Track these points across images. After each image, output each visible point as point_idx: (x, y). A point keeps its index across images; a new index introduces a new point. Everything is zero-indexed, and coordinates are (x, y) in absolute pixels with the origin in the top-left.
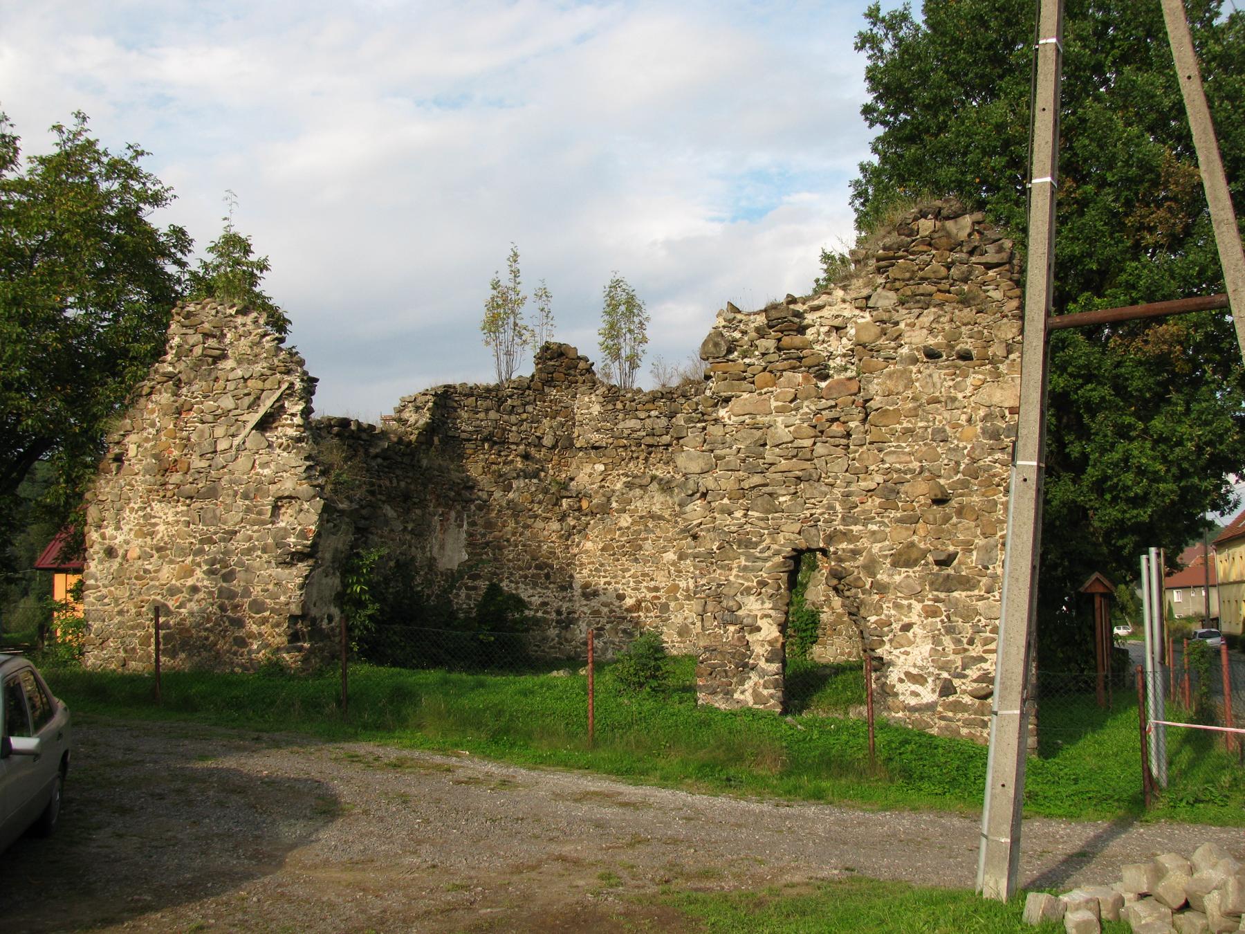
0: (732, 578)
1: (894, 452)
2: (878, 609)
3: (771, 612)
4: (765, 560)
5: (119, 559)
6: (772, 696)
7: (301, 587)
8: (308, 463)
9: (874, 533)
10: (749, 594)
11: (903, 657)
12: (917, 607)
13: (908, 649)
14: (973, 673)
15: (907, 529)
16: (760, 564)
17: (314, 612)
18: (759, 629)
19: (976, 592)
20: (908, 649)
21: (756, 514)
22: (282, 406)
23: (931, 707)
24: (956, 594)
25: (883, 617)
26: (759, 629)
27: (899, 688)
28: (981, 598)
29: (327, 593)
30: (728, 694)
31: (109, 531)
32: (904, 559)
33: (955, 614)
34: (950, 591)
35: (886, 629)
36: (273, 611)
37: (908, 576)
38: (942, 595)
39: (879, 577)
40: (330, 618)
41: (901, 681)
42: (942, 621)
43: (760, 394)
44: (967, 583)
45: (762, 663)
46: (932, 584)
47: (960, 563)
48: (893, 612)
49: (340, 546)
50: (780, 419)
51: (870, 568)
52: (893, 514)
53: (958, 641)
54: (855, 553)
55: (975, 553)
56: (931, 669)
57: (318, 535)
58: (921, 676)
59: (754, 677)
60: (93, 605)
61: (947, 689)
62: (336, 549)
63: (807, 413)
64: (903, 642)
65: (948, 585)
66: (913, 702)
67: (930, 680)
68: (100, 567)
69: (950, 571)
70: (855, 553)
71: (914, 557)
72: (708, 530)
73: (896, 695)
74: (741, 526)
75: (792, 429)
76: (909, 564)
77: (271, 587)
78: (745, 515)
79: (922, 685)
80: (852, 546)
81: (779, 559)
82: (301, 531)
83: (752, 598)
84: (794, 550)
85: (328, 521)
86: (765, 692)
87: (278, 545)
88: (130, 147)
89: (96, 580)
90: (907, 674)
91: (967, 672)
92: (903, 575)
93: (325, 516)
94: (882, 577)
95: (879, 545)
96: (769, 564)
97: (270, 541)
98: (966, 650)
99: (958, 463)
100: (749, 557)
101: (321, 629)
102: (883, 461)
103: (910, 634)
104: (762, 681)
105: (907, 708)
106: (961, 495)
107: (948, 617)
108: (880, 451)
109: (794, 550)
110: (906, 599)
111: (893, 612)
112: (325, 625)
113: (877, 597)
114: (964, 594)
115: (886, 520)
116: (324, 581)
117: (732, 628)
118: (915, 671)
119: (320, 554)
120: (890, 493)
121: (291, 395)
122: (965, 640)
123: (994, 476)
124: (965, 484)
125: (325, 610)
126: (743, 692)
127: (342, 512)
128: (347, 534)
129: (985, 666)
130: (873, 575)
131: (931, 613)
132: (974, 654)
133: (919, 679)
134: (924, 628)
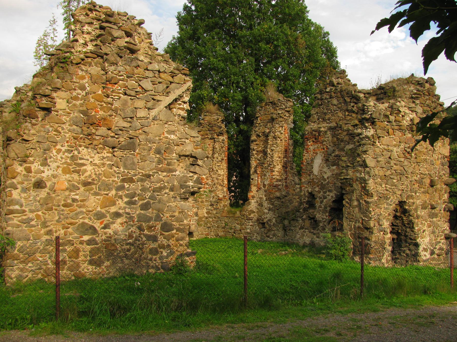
0: (382, 212)
2: (417, 224)
4: (391, 205)
5: (47, 190)
9: (418, 196)
19: (438, 219)
21: (389, 186)
23: (428, 260)
28: (439, 221)
30: (380, 260)
31: (35, 166)
32: (424, 208)
36: (178, 230)
38: (431, 220)
39: (418, 212)
43: (390, 138)
50: (395, 149)
51: (416, 210)
52: (422, 190)
54: (413, 203)
60: (18, 226)
61: (432, 253)
63: (402, 148)
66: (424, 258)
68: (23, 195)
69: (433, 211)
75: (398, 153)
76: (425, 208)
77: (176, 214)
78: (386, 187)
82: (198, 178)
83: (385, 220)
86: (389, 258)
87: (182, 187)
89: (21, 206)
91: (437, 247)
96: (391, 207)
97: (176, 183)
100: (387, 204)
103: (424, 234)
108: (419, 166)
114: (436, 219)
117: (382, 233)
120: (420, 182)
130: (416, 212)
131: (429, 226)
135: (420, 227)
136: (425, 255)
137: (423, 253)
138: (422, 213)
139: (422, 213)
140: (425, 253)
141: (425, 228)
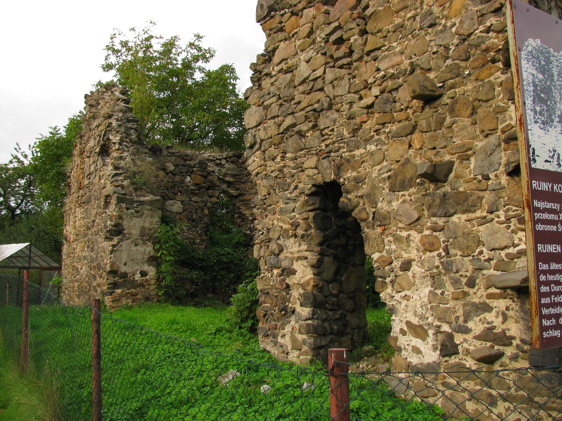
1: (386, 57)
3: (307, 254)
6: (304, 342)
8: (115, 172)
10: (289, 237)
11: (404, 303)
12: (415, 236)
13: (408, 293)
14: (476, 326)
15: (402, 143)
16: (291, 205)
17: (123, 269)
18: (294, 272)
19: (478, 214)
20: (408, 293)
22: (109, 139)
24: (455, 218)
25: (384, 253)
26: (294, 272)
27: (403, 341)
28: (484, 221)
29: (140, 257)
33: (454, 245)
34: (448, 215)
35: (387, 268)
37: (404, 201)
38: (441, 222)
39: (379, 205)
40: (144, 274)
41: (403, 332)
42: (439, 255)
44: (466, 203)
45: (298, 309)
46: (430, 207)
47: (457, 177)
48: (393, 247)
49: (147, 225)
53: (456, 282)
54: (359, 181)
55: (472, 159)
56: (430, 320)
58: (421, 326)
59: (293, 319)
61: (448, 348)
62: (143, 228)
64: (404, 284)
65: (446, 206)
66: (414, 360)
67: (431, 332)
69: (447, 188)
70: (359, 181)
71: (408, 176)
72: (262, 179)
73: (400, 350)
74: (281, 170)
79: (424, 339)
80: (355, 174)
81: (303, 198)
84: (314, 185)
88: (195, 36)
90: (408, 323)
91: (470, 325)
92: (401, 200)
93: (124, 205)
94: (382, 206)
95: (378, 167)
98: (465, 294)
99: (447, 48)
101: (134, 280)
102: (378, 70)
104: (297, 326)
105: (409, 367)
106: (453, 87)
107: (446, 250)
109: (314, 185)
110: (407, 230)
111: (393, 247)
112: (138, 277)
113: (379, 230)
114: (464, 217)
115: (383, 137)
116: (134, 248)
117: (276, 271)
118: (415, 321)
119: (126, 231)
120: (385, 105)
122: (464, 280)
123: (487, 50)
124: (455, 71)
125: (137, 267)
126: (283, 336)
127: (142, 203)
128: (152, 216)
129: (490, 316)
130: (374, 204)
132: (476, 300)
133: (419, 331)
134: (422, 266)
135: (389, 252)
136: (417, 350)
137: (407, 342)
138: (391, 203)
139: (391, 203)
140: (417, 342)
141: (414, 254)
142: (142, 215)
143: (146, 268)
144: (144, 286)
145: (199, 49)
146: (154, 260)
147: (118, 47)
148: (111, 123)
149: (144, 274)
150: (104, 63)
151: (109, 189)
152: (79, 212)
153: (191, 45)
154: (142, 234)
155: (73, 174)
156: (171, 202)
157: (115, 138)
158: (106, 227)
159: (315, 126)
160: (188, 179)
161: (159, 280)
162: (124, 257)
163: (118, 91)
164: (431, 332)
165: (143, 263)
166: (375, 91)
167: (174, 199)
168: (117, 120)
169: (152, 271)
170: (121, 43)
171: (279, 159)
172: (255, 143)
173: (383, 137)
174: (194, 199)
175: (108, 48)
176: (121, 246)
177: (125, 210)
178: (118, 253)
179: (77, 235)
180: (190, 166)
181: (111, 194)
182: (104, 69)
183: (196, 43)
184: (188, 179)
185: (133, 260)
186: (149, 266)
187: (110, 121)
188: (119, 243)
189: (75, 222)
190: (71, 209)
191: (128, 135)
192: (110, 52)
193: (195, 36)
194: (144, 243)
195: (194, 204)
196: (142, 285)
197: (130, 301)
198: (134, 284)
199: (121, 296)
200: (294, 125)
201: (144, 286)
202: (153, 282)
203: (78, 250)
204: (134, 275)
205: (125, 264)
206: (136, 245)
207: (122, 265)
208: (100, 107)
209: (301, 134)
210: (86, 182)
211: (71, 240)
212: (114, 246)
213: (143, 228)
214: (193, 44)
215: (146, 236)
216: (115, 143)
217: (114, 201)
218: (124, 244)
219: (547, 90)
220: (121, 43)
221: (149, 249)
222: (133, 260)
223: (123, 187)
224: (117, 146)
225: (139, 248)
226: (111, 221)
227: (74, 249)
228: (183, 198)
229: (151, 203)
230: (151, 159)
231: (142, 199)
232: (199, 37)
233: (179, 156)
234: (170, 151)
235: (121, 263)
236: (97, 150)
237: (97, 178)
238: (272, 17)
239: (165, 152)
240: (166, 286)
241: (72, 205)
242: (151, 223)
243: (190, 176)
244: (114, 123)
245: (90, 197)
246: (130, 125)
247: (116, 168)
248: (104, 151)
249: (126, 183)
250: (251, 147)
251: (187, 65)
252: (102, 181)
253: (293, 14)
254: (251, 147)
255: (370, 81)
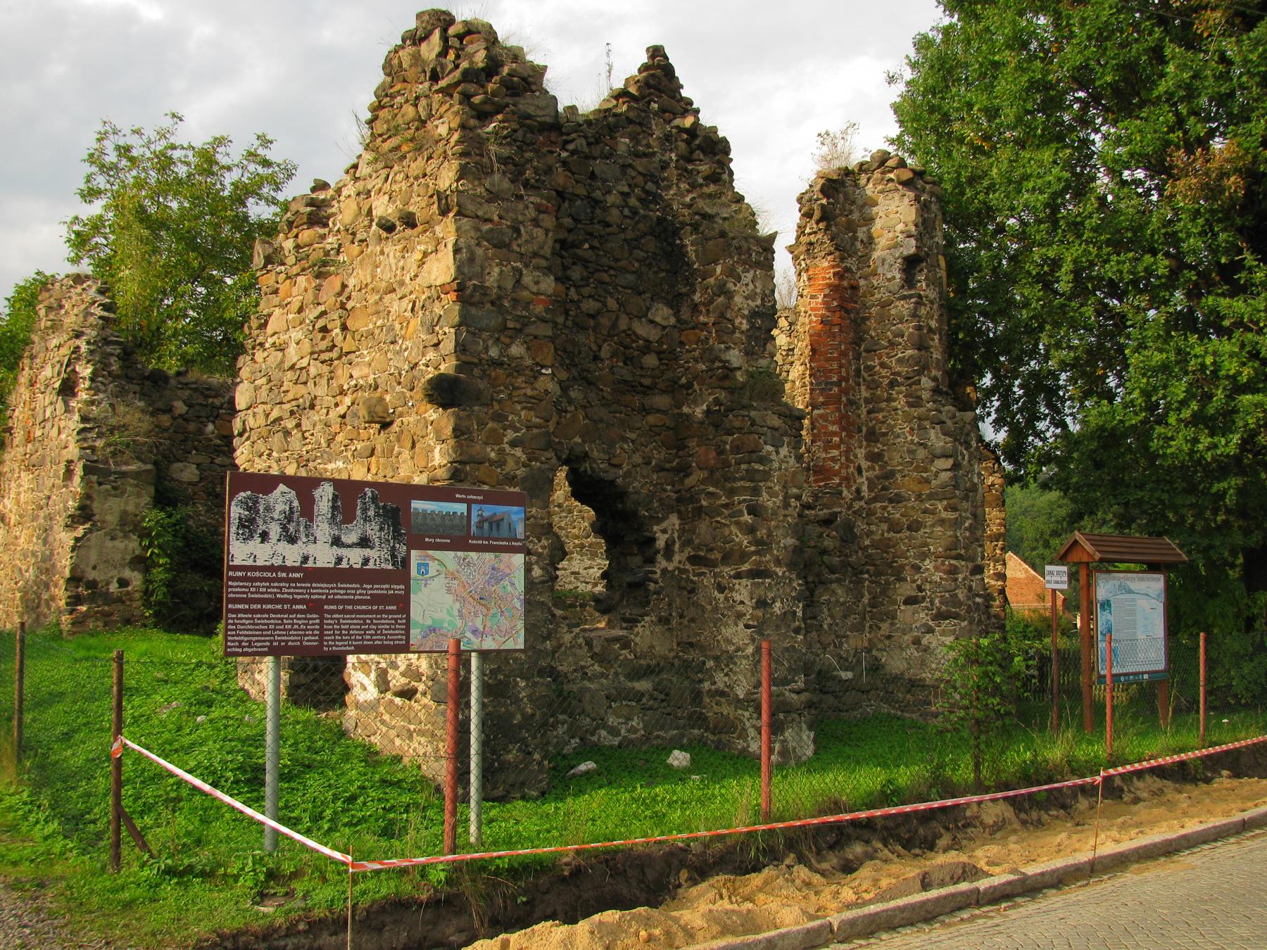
7: (73, 549)
17: (91, 575)
22: (74, 370)
40: (123, 583)
41: (355, 668)
49: (131, 508)
57: (87, 497)
62: (124, 513)
66: (361, 698)
85: (100, 484)
88: (259, 137)
93: (94, 478)
101: (107, 593)
105: (358, 705)
112: (114, 587)
116: (110, 544)
119: (97, 518)
121: (78, 359)
125: (114, 572)
127: (124, 475)
128: (139, 495)
142: (123, 492)
143: (127, 573)
144: (123, 602)
145: (266, 163)
146: (141, 563)
147: (112, 157)
148: (78, 347)
149: (123, 583)
150: (84, 187)
151: (73, 451)
152: (26, 477)
153: (251, 155)
154: (123, 521)
155: (16, 413)
156: (180, 465)
157: (85, 371)
158: (66, 509)
159: (298, 425)
160: (210, 427)
161: (147, 593)
162: (93, 557)
163: (94, 289)
164: (374, 667)
165: (123, 566)
166: (347, 401)
167: (185, 460)
168: (88, 343)
169: (136, 579)
170: (118, 148)
171: (265, 457)
172: (244, 430)
173: (349, 454)
174: (218, 460)
175: (92, 159)
176: (88, 540)
177: (96, 485)
178: (83, 551)
179: (21, 516)
180: (213, 406)
181: (75, 459)
182: (83, 196)
183: (261, 151)
184: (210, 427)
185: (107, 561)
186: (133, 570)
187: (78, 342)
188: (85, 534)
189: (19, 494)
190: (12, 471)
191: (106, 365)
192: (95, 169)
193: (259, 137)
194: (126, 536)
195: (219, 470)
196: (120, 600)
197: (100, 624)
198: (108, 598)
199: (86, 616)
200: (280, 419)
201: (123, 602)
202: (137, 595)
203: (22, 540)
204: (108, 584)
205: (94, 568)
206: (113, 539)
207: (90, 569)
208: (63, 312)
209: (287, 433)
210: (38, 433)
211: (12, 523)
212: (77, 539)
213: (124, 513)
214: (256, 156)
215: (129, 525)
216: (84, 378)
217: (79, 471)
218: (93, 536)
219: (252, 521)
220: (118, 148)
221: (133, 545)
222: (107, 561)
223: (93, 449)
224: (88, 383)
225: (117, 543)
226: (74, 500)
227: (16, 538)
228: (200, 459)
229: (137, 475)
230: (141, 404)
231: (124, 468)
232: (265, 142)
233: (196, 390)
234: (181, 379)
235: (87, 565)
236: (57, 385)
237: (55, 430)
238: (268, 272)
239: (173, 382)
240: (159, 603)
241: (16, 466)
242: (137, 505)
243: (213, 422)
244: (84, 348)
245: (44, 457)
246: (109, 349)
247: (84, 419)
248: (67, 389)
249: (99, 443)
250: (241, 435)
251: (243, 193)
252: (63, 436)
253: (288, 278)
254: (241, 435)
255: (345, 387)
